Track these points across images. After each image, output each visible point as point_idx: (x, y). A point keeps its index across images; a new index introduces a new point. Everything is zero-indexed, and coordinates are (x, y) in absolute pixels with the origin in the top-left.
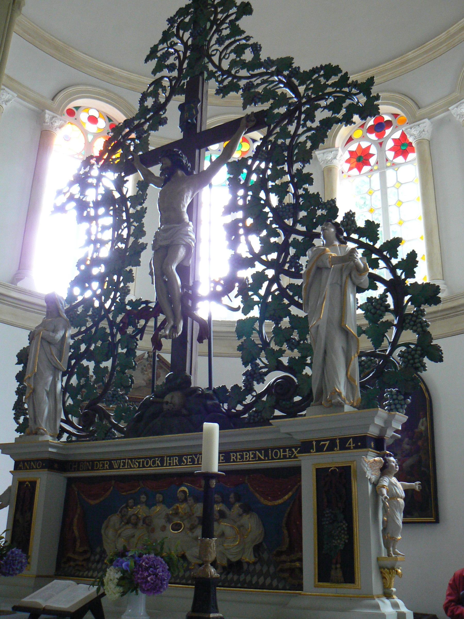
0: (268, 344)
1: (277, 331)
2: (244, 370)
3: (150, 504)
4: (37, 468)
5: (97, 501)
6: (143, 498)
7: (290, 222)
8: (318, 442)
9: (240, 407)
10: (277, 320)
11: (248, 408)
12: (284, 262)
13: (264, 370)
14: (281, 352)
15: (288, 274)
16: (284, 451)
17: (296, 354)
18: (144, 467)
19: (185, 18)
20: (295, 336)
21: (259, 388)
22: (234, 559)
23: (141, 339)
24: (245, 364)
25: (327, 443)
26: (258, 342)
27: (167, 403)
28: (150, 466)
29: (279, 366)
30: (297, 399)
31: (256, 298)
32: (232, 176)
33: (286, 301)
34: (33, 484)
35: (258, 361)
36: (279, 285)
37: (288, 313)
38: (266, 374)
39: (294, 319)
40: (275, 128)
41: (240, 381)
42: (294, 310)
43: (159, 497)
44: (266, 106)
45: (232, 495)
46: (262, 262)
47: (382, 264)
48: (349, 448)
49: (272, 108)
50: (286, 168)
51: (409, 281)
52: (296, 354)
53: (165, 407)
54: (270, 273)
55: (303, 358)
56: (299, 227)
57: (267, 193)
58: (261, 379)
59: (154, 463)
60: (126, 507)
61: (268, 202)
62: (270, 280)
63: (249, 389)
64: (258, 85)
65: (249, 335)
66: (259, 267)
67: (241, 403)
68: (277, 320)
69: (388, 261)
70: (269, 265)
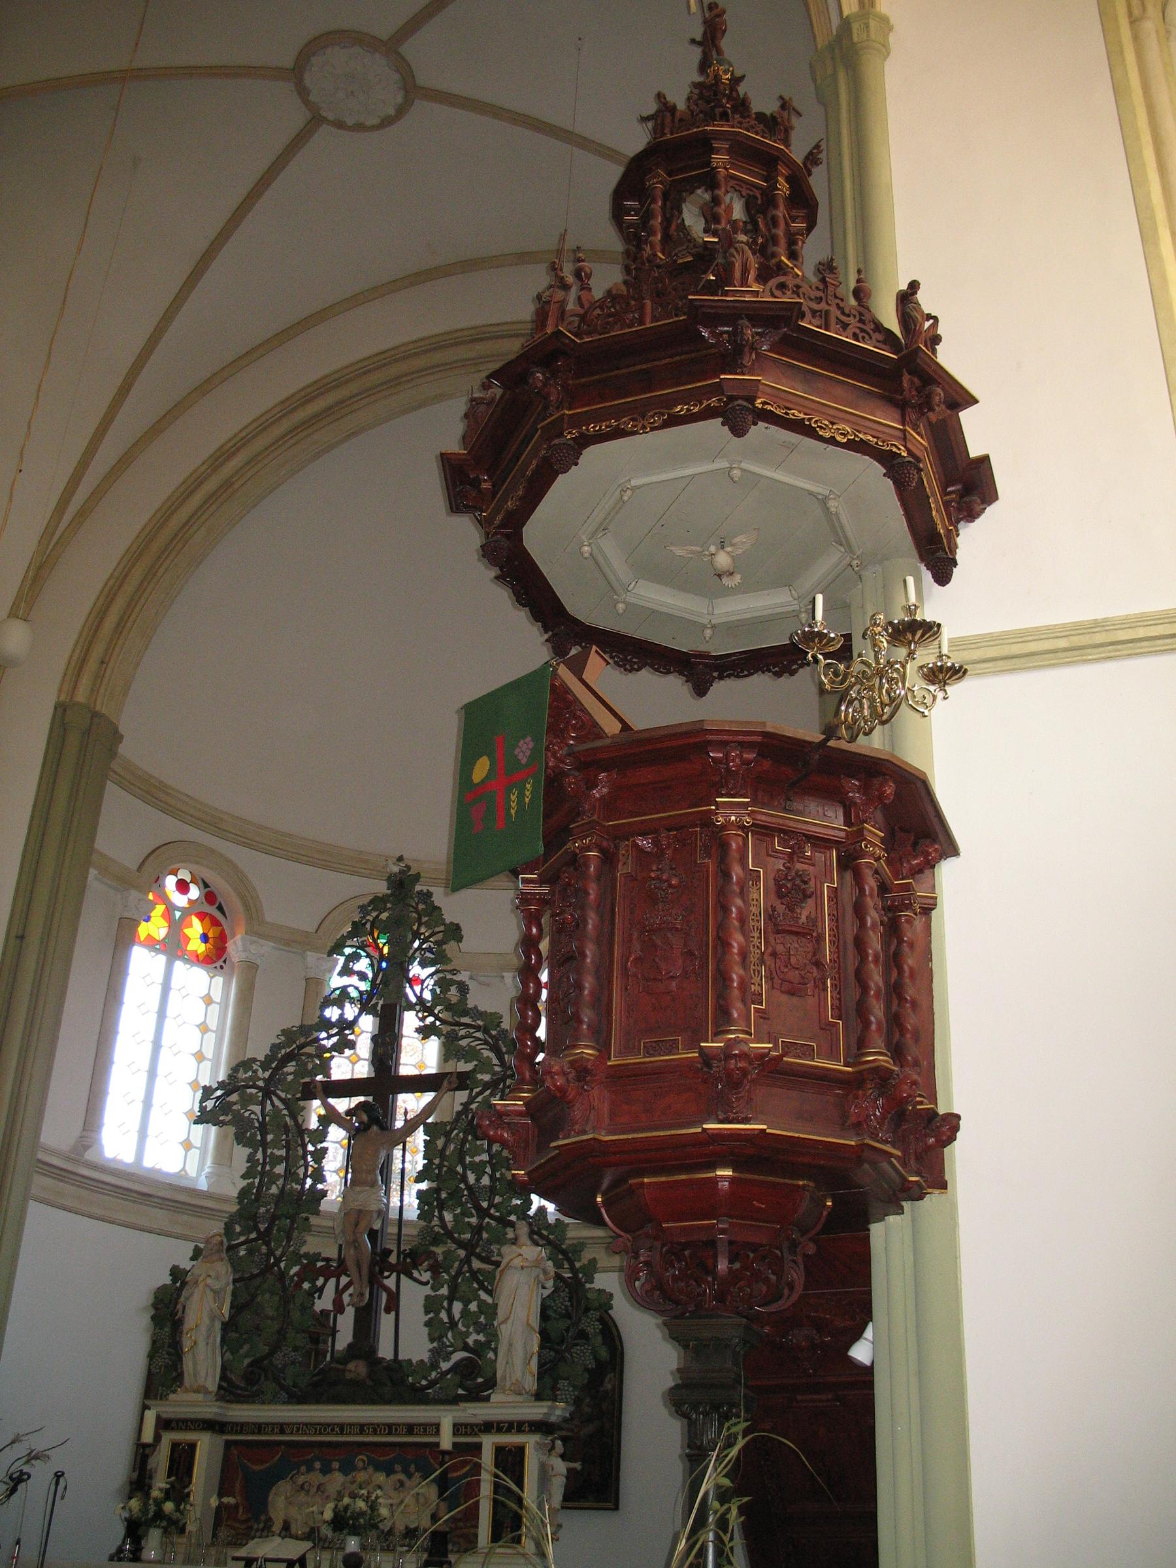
0: (456, 1324)
1: (465, 1313)
2: (431, 1346)
3: (326, 1470)
4: (195, 1429)
5: (263, 1467)
6: (318, 1465)
7: (485, 1204)
8: (499, 1423)
9: (424, 1382)
10: (466, 1304)
11: (432, 1384)
12: (477, 1245)
13: (451, 1349)
14: (468, 1334)
15: (479, 1258)
16: (466, 1428)
17: (481, 1338)
18: (320, 1433)
19: (381, 913)
20: (482, 1319)
21: (445, 1366)
22: (412, 1526)
23: (319, 1298)
24: (432, 1340)
25: (506, 1425)
26: (446, 1320)
27: (350, 1371)
28: (328, 1433)
29: (466, 1347)
30: (480, 1380)
31: (446, 1277)
32: (428, 1138)
33: (475, 1285)
34: (192, 1446)
35: (445, 1340)
36: (470, 1267)
37: (478, 1298)
38: (452, 1353)
39: (482, 1304)
40: (479, 1094)
41: (425, 1356)
42: (483, 1295)
43: (336, 1465)
44: (469, 1067)
45: (413, 1466)
46: (454, 1241)
47: (566, 1266)
48: (524, 1431)
49: (474, 1071)
50: (486, 1147)
51: (588, 1286)
52: (481, 1338)
53: (348, 1376)
54: (462, 1253)
55: (489, 1342)
56: (492, 1211)
57: (465, 1168)
58: (447, 1358)
59: (333, 1430)
60: (297, 1474)
61: (464, 1178)
62: (461, 1261)
63: (434, 1365)
64: (463, 1037)
65: (437, 1313)
66: (452, 1246)
67: (426, 1379)
68: (466, 1304)
69: (571, 1263)
70: (461, 1244)
